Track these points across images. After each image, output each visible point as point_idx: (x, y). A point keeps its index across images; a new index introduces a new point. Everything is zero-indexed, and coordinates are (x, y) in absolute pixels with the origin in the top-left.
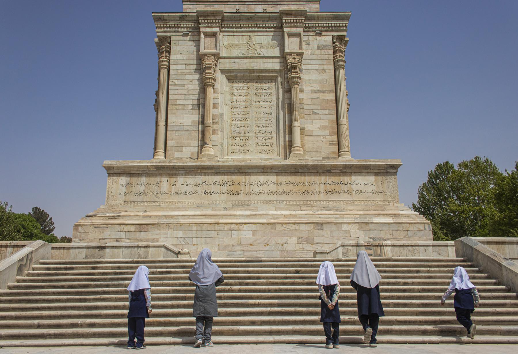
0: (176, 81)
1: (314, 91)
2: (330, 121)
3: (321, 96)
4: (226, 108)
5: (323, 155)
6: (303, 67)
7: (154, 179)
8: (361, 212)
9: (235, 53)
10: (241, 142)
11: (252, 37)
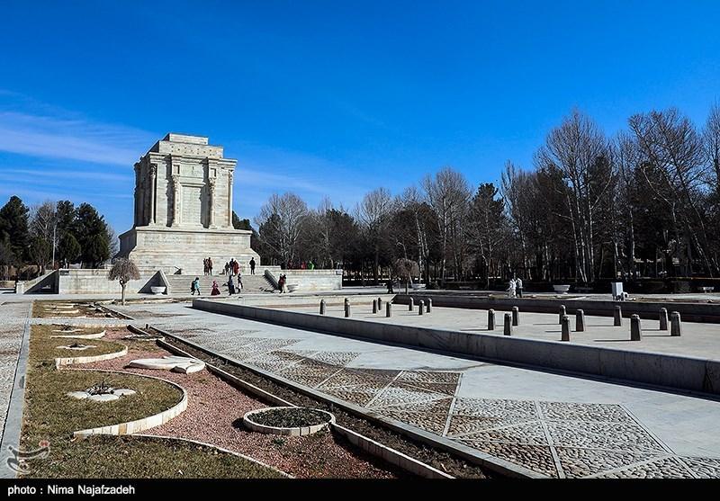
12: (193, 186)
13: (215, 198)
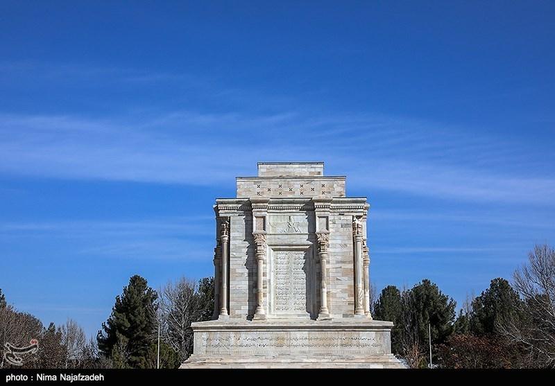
0: (234, 254)
1: (338, 262)
2: (350, 286)
3: (343, 266)
4: (272, 273)
5: (343, 312)
6: (330, 242)
7: (225, 335)
8: (363, 361)
9: (279, 230)
10: (284, 302)
11: (291, 217)
12: (291, 248)
13: (330, 265)
